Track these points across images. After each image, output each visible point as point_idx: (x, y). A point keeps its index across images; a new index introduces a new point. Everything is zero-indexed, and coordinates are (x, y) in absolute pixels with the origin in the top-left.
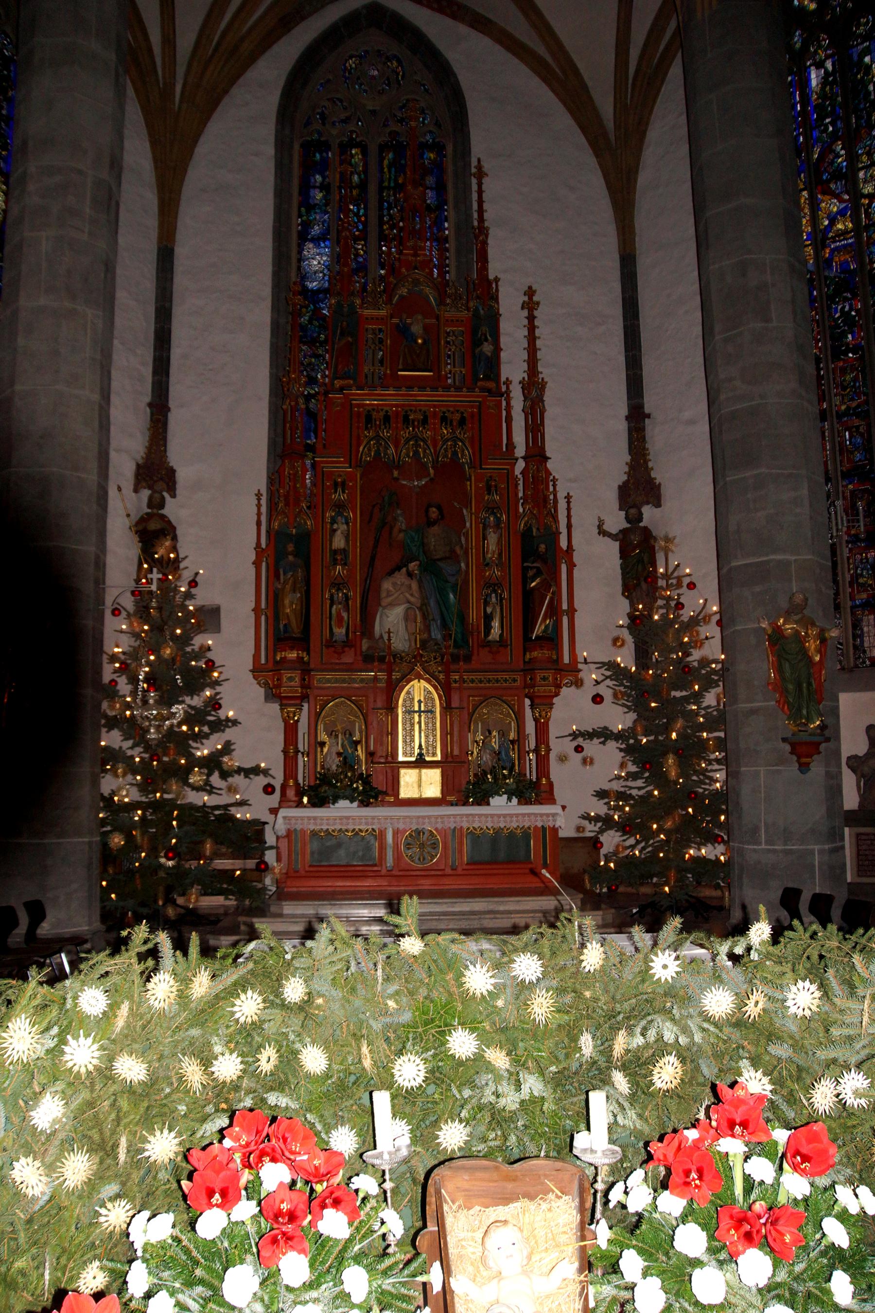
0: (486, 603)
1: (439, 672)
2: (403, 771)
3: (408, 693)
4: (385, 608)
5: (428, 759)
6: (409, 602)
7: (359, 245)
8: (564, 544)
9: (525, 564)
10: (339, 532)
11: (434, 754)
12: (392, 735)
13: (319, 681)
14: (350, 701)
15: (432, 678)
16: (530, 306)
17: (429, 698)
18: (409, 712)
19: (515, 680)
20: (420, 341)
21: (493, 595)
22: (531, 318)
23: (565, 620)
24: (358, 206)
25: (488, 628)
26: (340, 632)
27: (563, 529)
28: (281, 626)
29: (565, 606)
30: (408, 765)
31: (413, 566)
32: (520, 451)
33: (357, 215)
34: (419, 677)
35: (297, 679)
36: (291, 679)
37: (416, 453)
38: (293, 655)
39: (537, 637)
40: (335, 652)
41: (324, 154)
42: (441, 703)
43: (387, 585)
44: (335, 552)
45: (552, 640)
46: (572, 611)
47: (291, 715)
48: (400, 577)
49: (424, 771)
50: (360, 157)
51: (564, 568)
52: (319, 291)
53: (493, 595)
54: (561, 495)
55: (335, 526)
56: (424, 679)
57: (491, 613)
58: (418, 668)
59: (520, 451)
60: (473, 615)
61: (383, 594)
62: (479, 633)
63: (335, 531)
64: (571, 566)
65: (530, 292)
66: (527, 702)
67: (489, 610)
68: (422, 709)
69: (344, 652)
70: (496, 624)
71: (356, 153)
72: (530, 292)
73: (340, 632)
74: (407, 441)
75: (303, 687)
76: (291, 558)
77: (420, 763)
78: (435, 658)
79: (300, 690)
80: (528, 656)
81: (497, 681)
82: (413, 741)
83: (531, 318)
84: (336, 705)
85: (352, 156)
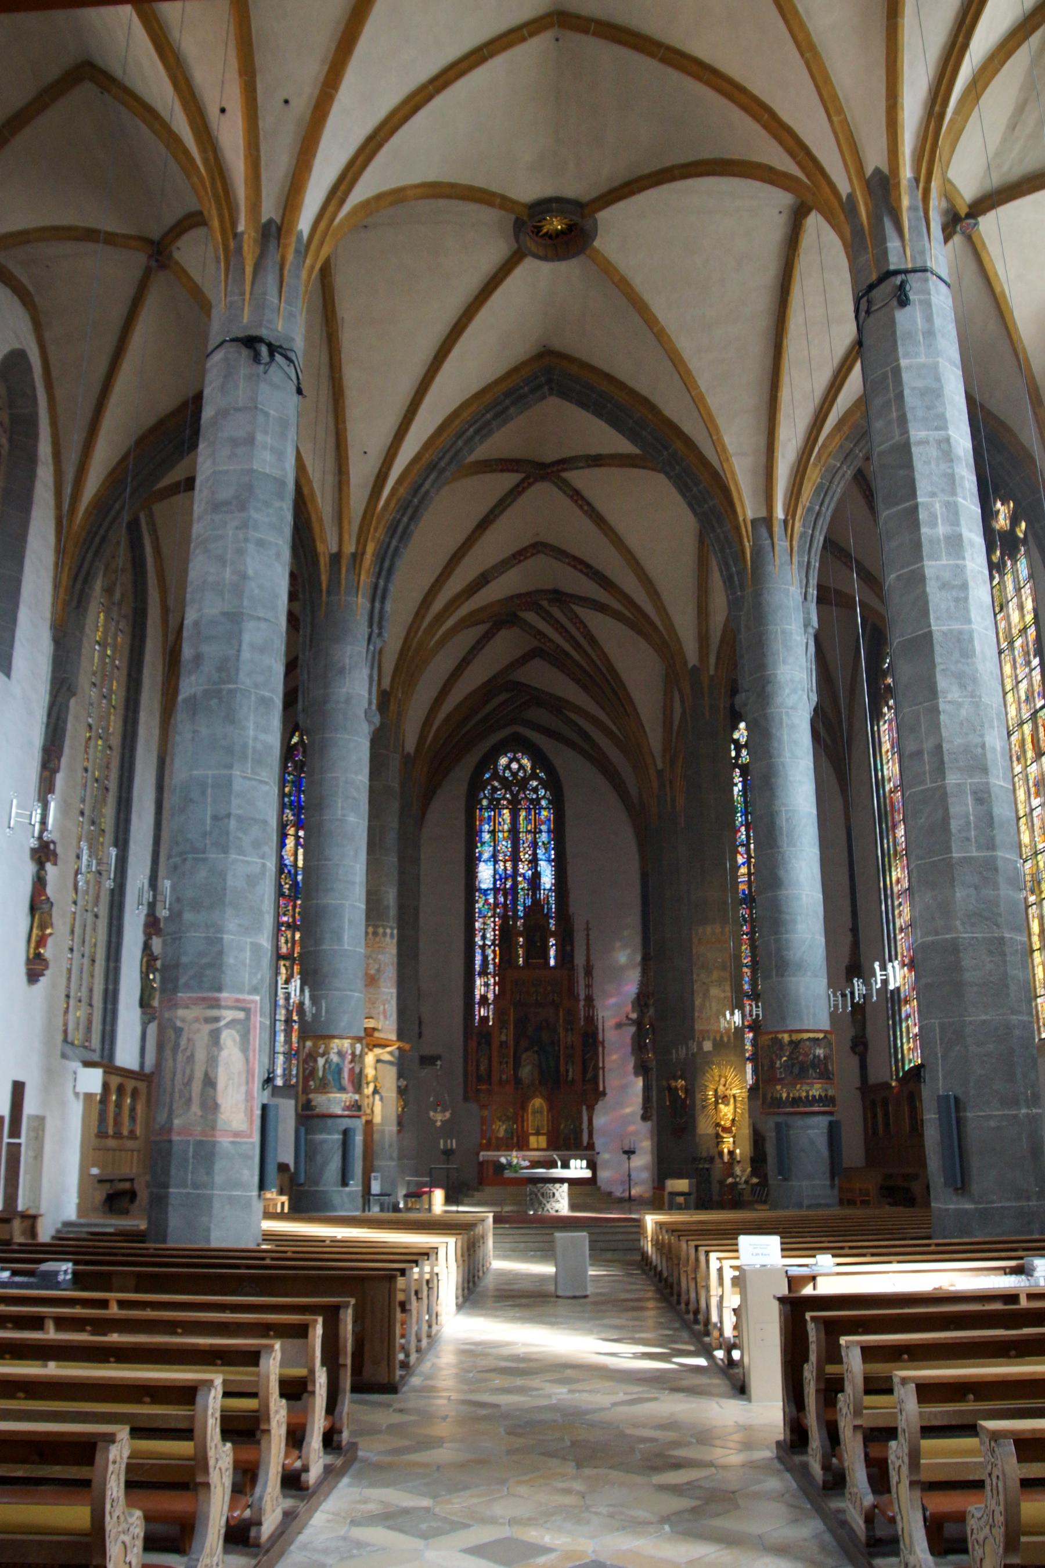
0: (567, 1063)
8: (600, 1038)
15: (543, 1097)
16: (588, 929)
17: (542, 1107)
18: (534, 1113)
23: (601, 1072)
25: (567, 1076)
26: (504, 1077)
27: (600, 1031)
29: (601, 1065)
30: (533, 1134)
31: (536, 1048)
32: (582, 996)
38: (484, 1087)
43: (524, 1056)
44: (502, 1043)
45: (595, 1080)
46: (603, 1068)
48: (529, 1053)
51: (600, 1049)
52: (487, 890)
54: (600, 1017)
59: (582, 996)
60: (562, 1069)
64: (604, 1048)
65: (587, 923)
66: (584, 1107)
70: (570, 1074)
72: (587, 923)
73: (504, 1077)
77: (538, 1133)
83: (588, 935)
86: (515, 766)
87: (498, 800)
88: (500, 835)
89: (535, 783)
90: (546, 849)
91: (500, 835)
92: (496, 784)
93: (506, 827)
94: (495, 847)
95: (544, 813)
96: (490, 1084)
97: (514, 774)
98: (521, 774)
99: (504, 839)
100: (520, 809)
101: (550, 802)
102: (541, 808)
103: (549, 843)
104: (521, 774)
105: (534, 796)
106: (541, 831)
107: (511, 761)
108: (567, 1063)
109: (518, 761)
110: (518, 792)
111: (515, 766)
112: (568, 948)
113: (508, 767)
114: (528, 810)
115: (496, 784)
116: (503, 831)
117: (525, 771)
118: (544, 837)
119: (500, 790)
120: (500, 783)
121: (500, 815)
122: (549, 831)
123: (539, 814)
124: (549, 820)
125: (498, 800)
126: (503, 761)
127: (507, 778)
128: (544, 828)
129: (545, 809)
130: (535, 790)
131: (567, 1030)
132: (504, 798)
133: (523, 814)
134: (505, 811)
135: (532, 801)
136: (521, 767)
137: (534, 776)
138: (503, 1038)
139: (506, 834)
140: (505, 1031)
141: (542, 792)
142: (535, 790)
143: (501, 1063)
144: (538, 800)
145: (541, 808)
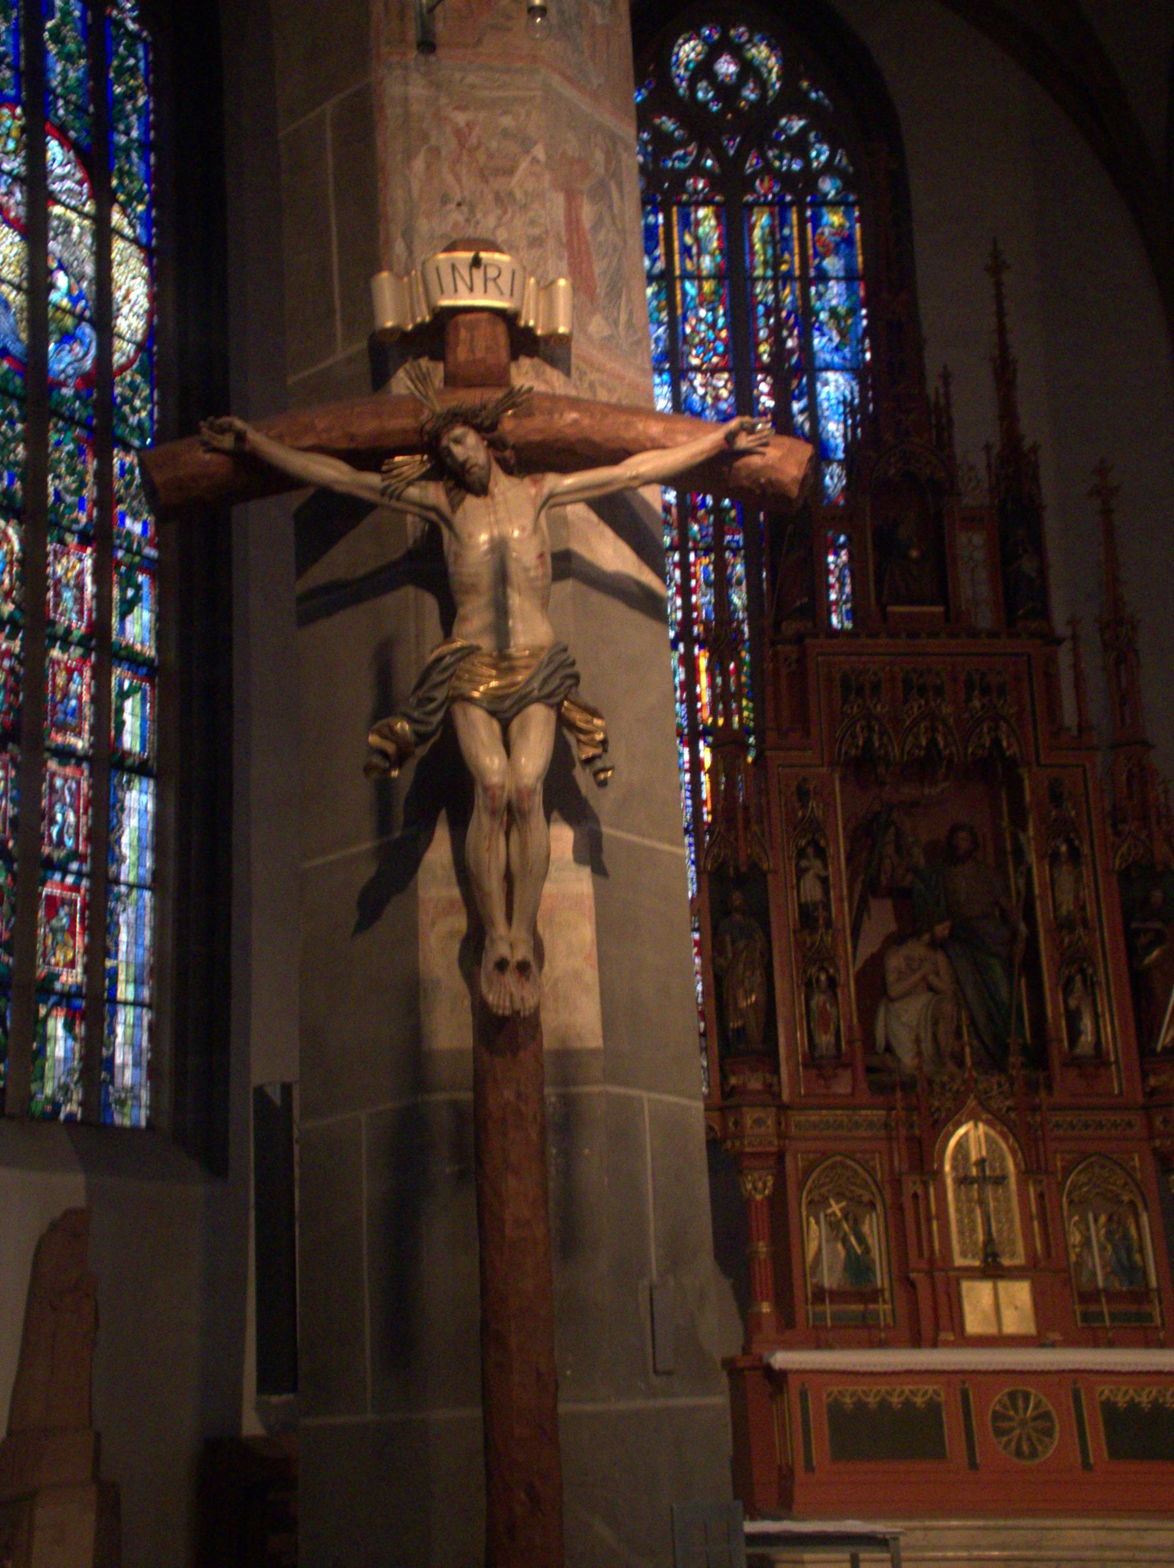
0: (1067, 989)
1: (1009, 1109)
2: (965, 1285)
3: (959, 1144)
4: (892, 1000)
5: (1006, 1262)
6: (931, 988)
7: (720, 380)
9: (1134, 925)
10: (812, 872)
11: (1013, 1254)
12: (938, 1219)
13: (798, 1125)
14: (855, 1160)
15: (997, 1119)
18: (963, 1181)
19: (1130, 1125)
20: (914, 554)
21: (1078, 978)
22: (1107, 513)
24: (713, 310)
25: (1074, 1034)
26: (825, 1040)
28: (730, 1034)
33: (712, 326)
34: (975, 1117)
35: (769, 1122)
36: (759, 1122)
37: (933, 742)
39: (1164, 1048)
40: (820, 1076)
41: (651, 219)
42: (1016, 1165)
47: (760, 1185)
48: (916, 949)
49: (1002, 1285)
50: (713, 222)
53: (1078, 978)
55: (804, 863)
56: (982, 1121)
57: (1078, 1008)
58: (971, 1102)
61: (891, 978)
62: (1061, 1041)
63: (807, 870)
67: (1073, 1003)
68: (988, 1172)
69: (835, 1076)
71: (705, 217)
72: (1102, 470)
73: (825, 1040)
74: (916, 723)
75: (781, 1136)
76: (738, 917)
78: (1000, 1085)
79: (776, 1142)
80: (1152, 1081)
81: (1100, 1125)
82: (973, 1230)
83: (1107, 513)
84: (833, 1166)
85: (698, 223)
86: (726, 67)
87: (679, 178)
88: (691, 288)
89: (797, 125)
90: (842, 333)
91: (691, 288)
92: (668, 124)
93: (707, 263)
94: (673, 326)
95: (834, 219)
96: (776, 1071)
97: (727, 92)
98: (750, 93)
99: (702, 300)
100: (750, 207)
101: (849, 183)
102: (821, 202)
103: (853, 311)
104: (750, 93)
105: (796, 167)
106: (823, 277)
107: (713, 52)
108: (1067, 989)
109: (737, 53)
110: (741, 155)
111: (726, 67)
112: (1028, 566)
113: (704, 70)
114: (779, 210)
115: (668, 124)
116: (697, 277)
117: (762, 85)
118: (835, 294)
119: (683, 144)
120: (682, 122)
121: (688, 223)
122: (849, 277)
123: (816, 221)
124: (848, 240)
125: (679, 178)
126: (688, 51)
127: (706, 104)
128: (832, 264)
129: (834, 205)
130: (799, 146)
131: (1054, 858)
132: (697, 170)
133: (762, 221)
134: (702, 213)
135: (787, 180)
136: (748, 70)
137: (792, 101)
138: (811, 890)
139: (708, 287)
140: (818, 863)
141: (820, 154)
142: (799, 146)
143: (809, 986)
144: (809, 177)
145: (821, 202)
